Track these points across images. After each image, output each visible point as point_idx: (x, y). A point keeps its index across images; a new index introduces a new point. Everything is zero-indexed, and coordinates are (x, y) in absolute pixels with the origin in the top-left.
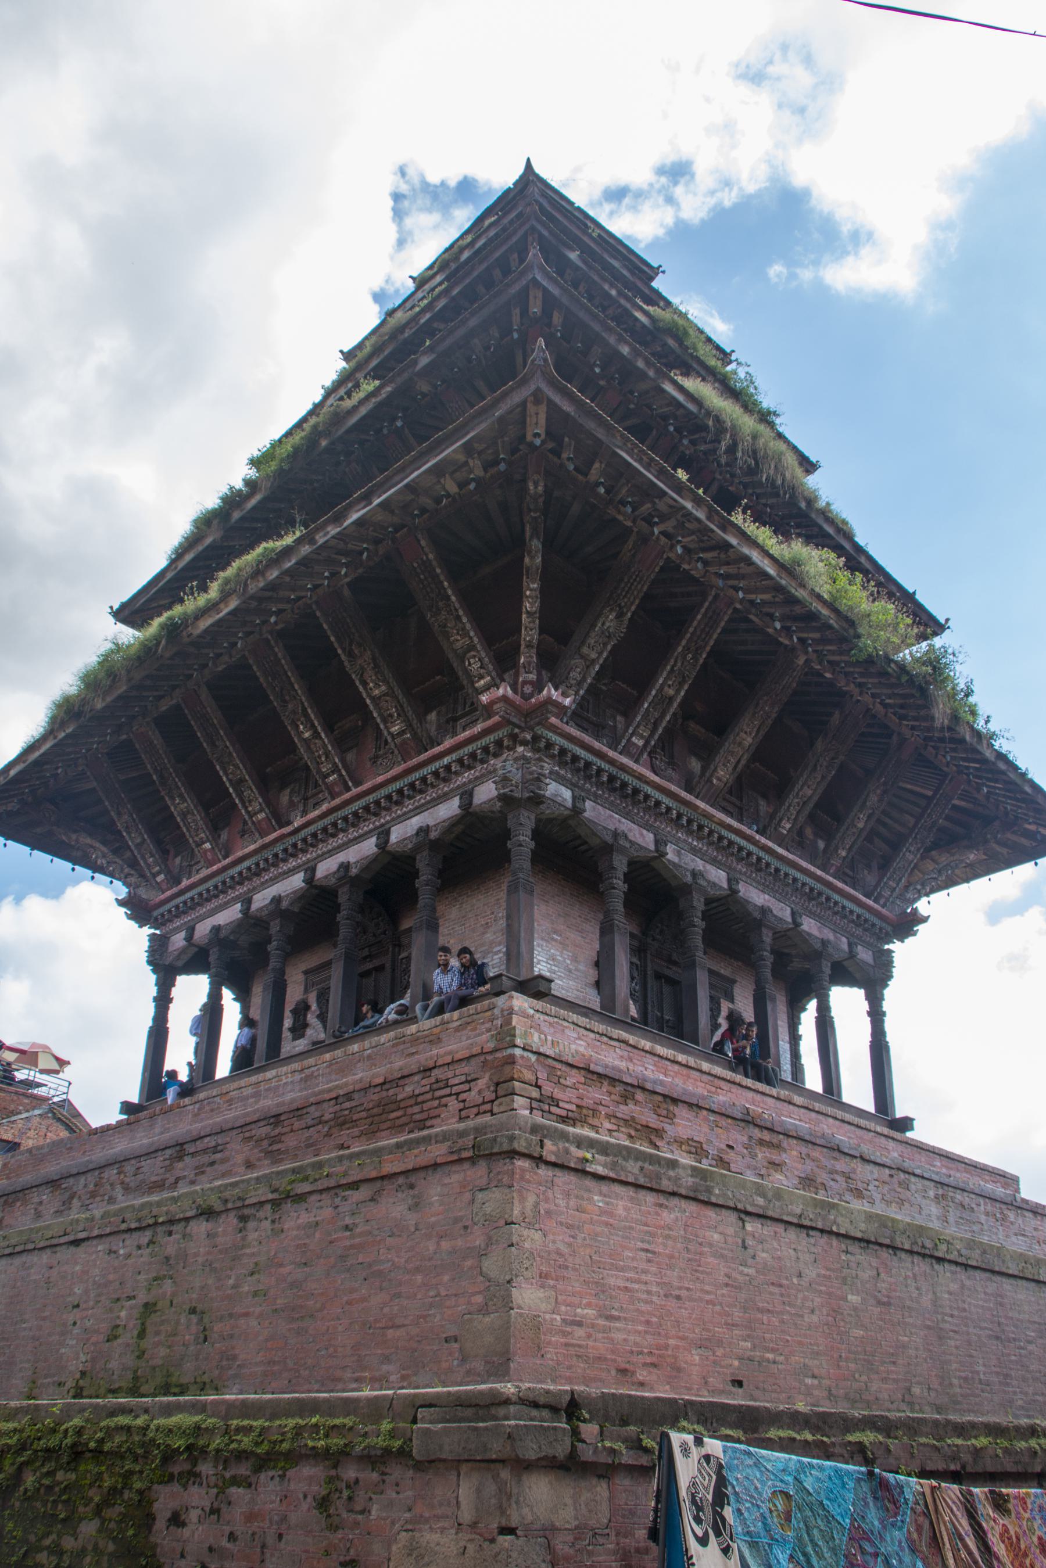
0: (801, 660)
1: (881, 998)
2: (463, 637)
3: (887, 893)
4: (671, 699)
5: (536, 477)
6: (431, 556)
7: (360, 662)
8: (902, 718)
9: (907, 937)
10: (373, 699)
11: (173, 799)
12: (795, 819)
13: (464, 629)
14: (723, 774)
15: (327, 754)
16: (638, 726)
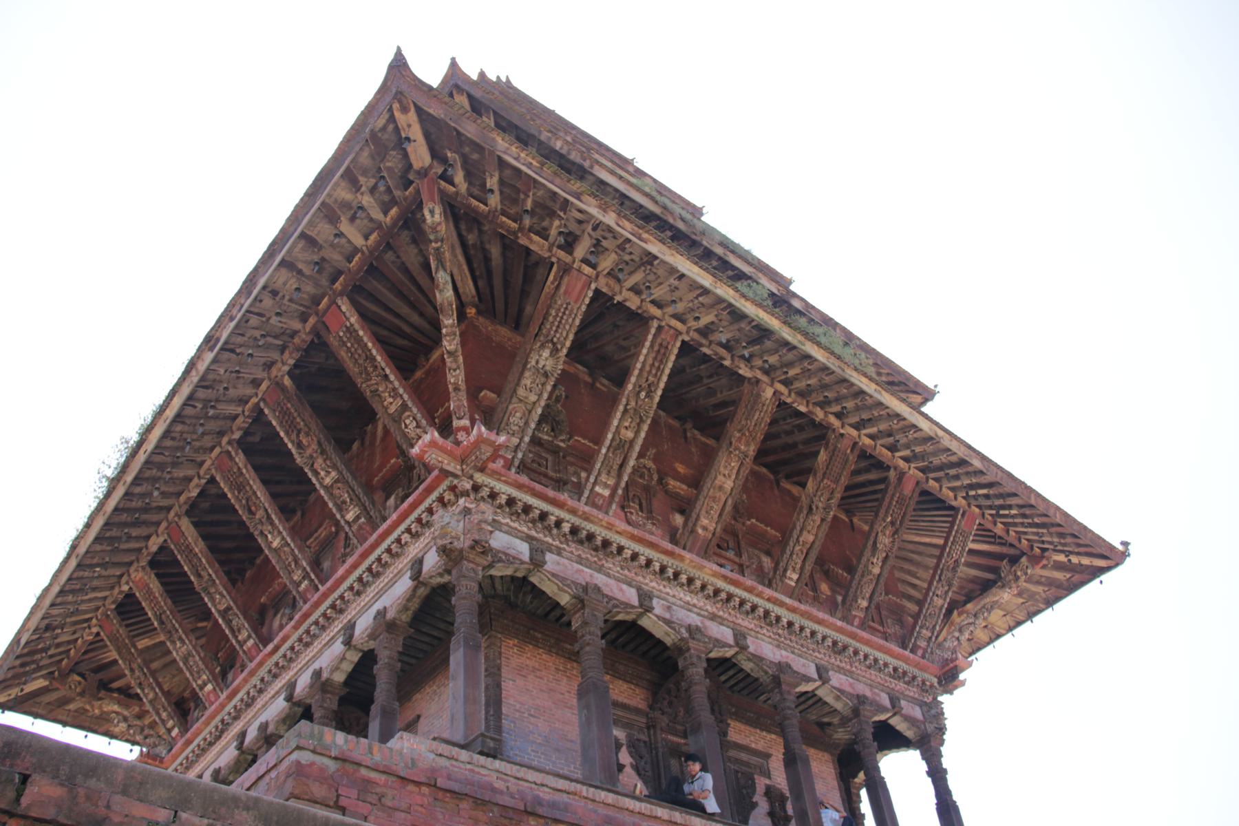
0: (769, 393)
2: (391, 394)
3: (923, 644)
4: (632, 442)
5: (431, 205)
6: (353, 320)
7: (309, 451)
8: (893, 448)
9: (956, 687)
10: (326, 488)
11: (173, 642)
12: (802, 568)
13: (394, 389)
14: (707, 523)
15: (296, 561)
16: (599, 474)
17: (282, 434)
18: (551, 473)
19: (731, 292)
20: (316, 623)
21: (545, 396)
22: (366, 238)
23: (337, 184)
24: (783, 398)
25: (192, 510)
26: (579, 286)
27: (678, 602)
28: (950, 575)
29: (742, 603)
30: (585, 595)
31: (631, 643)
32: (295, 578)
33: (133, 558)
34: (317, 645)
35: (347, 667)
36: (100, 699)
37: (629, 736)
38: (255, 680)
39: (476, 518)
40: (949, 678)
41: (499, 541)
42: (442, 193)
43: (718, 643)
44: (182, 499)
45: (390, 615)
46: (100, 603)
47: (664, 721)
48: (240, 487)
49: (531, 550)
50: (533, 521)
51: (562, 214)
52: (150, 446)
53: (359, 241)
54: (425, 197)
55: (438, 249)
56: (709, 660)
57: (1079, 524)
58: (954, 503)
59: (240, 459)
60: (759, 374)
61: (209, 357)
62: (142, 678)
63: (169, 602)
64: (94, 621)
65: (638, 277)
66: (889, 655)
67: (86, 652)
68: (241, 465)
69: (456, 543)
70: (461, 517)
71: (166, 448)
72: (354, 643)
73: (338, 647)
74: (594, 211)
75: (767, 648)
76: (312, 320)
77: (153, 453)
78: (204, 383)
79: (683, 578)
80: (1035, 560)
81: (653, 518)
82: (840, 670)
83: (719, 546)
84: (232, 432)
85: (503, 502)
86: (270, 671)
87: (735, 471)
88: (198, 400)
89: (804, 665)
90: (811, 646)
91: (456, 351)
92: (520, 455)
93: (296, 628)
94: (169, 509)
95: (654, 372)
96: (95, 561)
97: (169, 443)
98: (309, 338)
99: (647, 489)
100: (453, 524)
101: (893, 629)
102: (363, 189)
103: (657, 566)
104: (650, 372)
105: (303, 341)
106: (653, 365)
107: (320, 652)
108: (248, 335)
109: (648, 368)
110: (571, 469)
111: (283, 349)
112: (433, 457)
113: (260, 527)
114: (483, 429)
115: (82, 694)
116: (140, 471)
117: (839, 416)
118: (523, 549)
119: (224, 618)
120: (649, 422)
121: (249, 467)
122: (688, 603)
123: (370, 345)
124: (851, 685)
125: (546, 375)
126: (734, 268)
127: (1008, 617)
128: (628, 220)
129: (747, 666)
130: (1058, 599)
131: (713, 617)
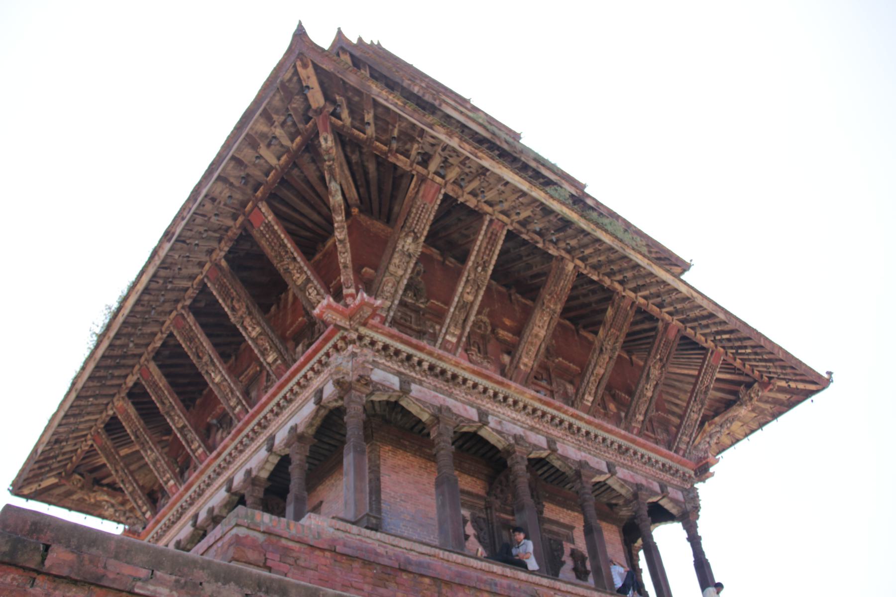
0: (570, 267)
1: (696, 526)
2: (298, 271)
3: (683, 446)
4: (472, 303)
5: (325, 134)
7: (240, 313)
8: (660, 306)
9: (708, 477)
10: (253, 339)
11: (146, 451)
12: (596, 393)
13: (301, 268)
14: (527, 361)
15: (232, 391)
16: (449, 327)
17: (220, 301)
18: (415, 327)
19: (543, 194)
20: (247, 436)
21: (409, 271)
22: (279, 159)
23: (257, 121)
24: (581, 270)
25: (157, 356)
26: (433, 191)
27: (507, 418)
28: (702, 396)
29: (553, 418)
30: (440, 414)
34: (248, 452)
35: (270, 467)
36: (95, 491)
37: (473, 515)
38: (204, 477)
39: (360, 359)
40: (702, 471)
41: (377, 375)
42: (333, 126)
43: (536, 447)
44: (150, 348)
45: (300, 430)
46: (93, 424)
47: (497, 503)
48: (191, 339)
49: (401, 381)
50: (402, 361)
51: (419, 139)
52: (126, 311)
53: (273, 161)
54: (320, 128)
55: (330, 166)
56: (529, 460)
57: (796, 359)
58: (705, 345)
59: (191, 319)
60: (563, 254)
61: (167, 246)
62: (124, 476)
63: (142, 422)
64: (89, 436)
65: (475, 184)
66: (659, 455)
67: (84, 459)
68: (191, 324)
69: (346, 378)
70: (350, 359)
71: (138, 312)
72: (274, 450)
73: (263, 453)
74: (443, 137)
75: (571, 450)
76: (241, 219)
77: (128, 316)
78: (164, 265)
79: (510, 401)
80: (764, 385)
81: (488, 358)
82: (624, 466)
83: (536, 378)
84: (185, 300)
85: (380, 348)
86: (215, 471)
88: (160, 277)
89: (598, 463)
90: (603, 449)
91: (345, 239)
92: (392, 314)
93: (233, 440)
94: (140, 356)
96: (89, 393)
97: (139, 308)
98: (239, 232)
99: (483, 337)
100: (344, 363)
101: (662, 436)
102: (276, 123)
103: (491, 392)
104: (484, 253)
105: (235, 234)
106: (486, 248)
107: (251, 457)
109: (483, 250)
110: (428, 323)
111: (220, 240)
112: (329, 316)
113: (205, 368)
114: (365, 295)
115: (82, 488)
116: (120, 329)
117: (621, 282)
119: (181, 433)
120: (484, 288)
121: (197, 325)
122: (514, 419)
123: (282, 236)
124: (632, 476)
125: (410, 256)
126: (544, 177)
127: (745, 427)
128: (468, 143)
129: (557, 464)
130: (781, 413)
131: (532, 429)
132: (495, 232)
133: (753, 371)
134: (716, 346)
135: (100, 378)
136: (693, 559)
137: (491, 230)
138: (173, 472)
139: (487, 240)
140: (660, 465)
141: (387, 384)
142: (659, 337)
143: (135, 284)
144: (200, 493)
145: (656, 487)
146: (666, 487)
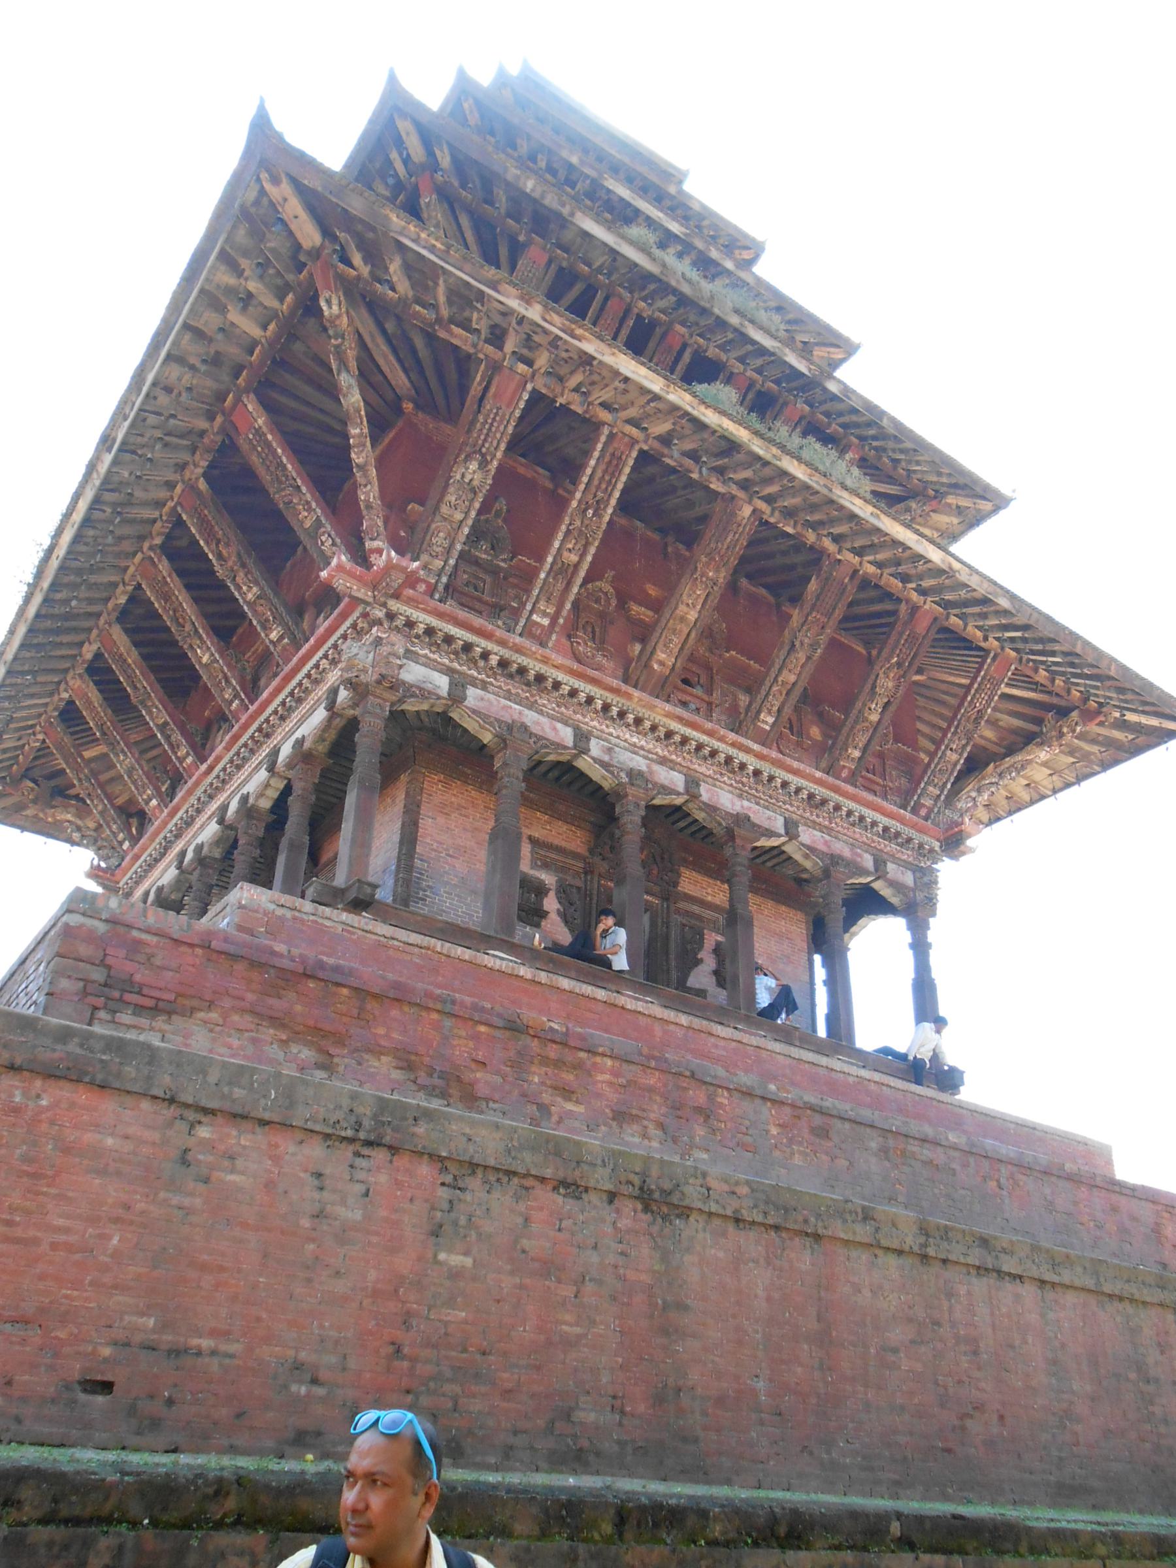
0: (747, 511)
1: (926, 927)
3: (928, 802)
4: (577, 566)
5: (327, 294)
7: (230, 563)
8: (905, 579)
9: (963, 853)
10: (248, 603)
12: (779, 711)
14: (664, 658)
17: (202, 543)
18: (486, 598)
19: (688, 397)
20: (245, 745)
21: (473, 514)
22: (265, 328)
23: (213, 267)
24: (765, 517)
25: (123, 616)
26: (513, 386)
27: (622, 744)
28: (970, 726)
29: (700, 747)
30: (511, 731)
31: (561, 784)
32: (227, 696)
33: (68, 665)
34: (247, 769)
35: (273, 794)
38: (193, 800)
39: (385, 650)
41: (413, 673)
42: (341, 278)
43: (666, 790)
44: (110, 605)
45: (307, 745)
46: (42, 710)
47: (603, 867)
48: (166, 597)
49: (451, 684)
50: (456, 653)
51: (479, 305)
52: (61, 551)
53: (256, 332)
54: (319, 284)
55: (337, 347)
56: (651, 808)
57: (1143, 679)
58: (983, 644)
59: (164, 566)
60: (734, 490)
61: (108, 458)
63: (109, 711)
64: (38, 728)
65: (577, 378)
67: (35, 758)
68: (165, 573)
69: (362, 677)
72: (276, 770)
73: (263, 774)
74: (514, 304)
75: (725, 798)
76: (219, 419)
77: (65, 558)
78: (108, 485)
79: (630, 718)
80: (1089, 716)
81: (603, 649)
82: (815, 825)
83: (686, 681)
84: (153, 538)
85: (421, 632)
86: (205, 791)
87: (701, 601)
88: (104, 503)
89: (769, 818)
90: (781, 798)
91: (366, 463)
92: (444, 579)
94: (98, 615)
95: (604, 486)
96: (26, 668)
97: (82, 548)
98: (219, 438)
99: (602, 615)
100: (362, 655)
102: (246, 274)
103: (599, 704)
104: (598, 487)
105: (212, 441)
107: (250, 776)
108: (148, 435)
109: (596, 482)
110: (512, 592)
111: (193, 450)
112: (341, 583)
114: (393, 553)
115: (35, 801)
116: (56, 576)
117: (837, 539)
118: (442, 683)
119: (162, 733)
120: (596, 544)
121: (174, 575)
122: (634, 745)
123: (279, 451)
124: (826, 843)
125: (474, 491)
126: (754, 342)
127: (1055, 778)
128: (558, 313)
129: (700, 816)
130: (1116, 762)
131: (663, 761)
132: (618, 453)
133: (1069, 692)
134: (1002, 648)
135: (39, 647)
136: (913, 975)
137: (611, 450)
138: (157, 789)
139: (602, 467)
140: (880, 829)
141: (429, 686)
142: (898, 627)
143: (67, 516)
144: (189, 822)
145: (868, 861)
146: (885, 863)
